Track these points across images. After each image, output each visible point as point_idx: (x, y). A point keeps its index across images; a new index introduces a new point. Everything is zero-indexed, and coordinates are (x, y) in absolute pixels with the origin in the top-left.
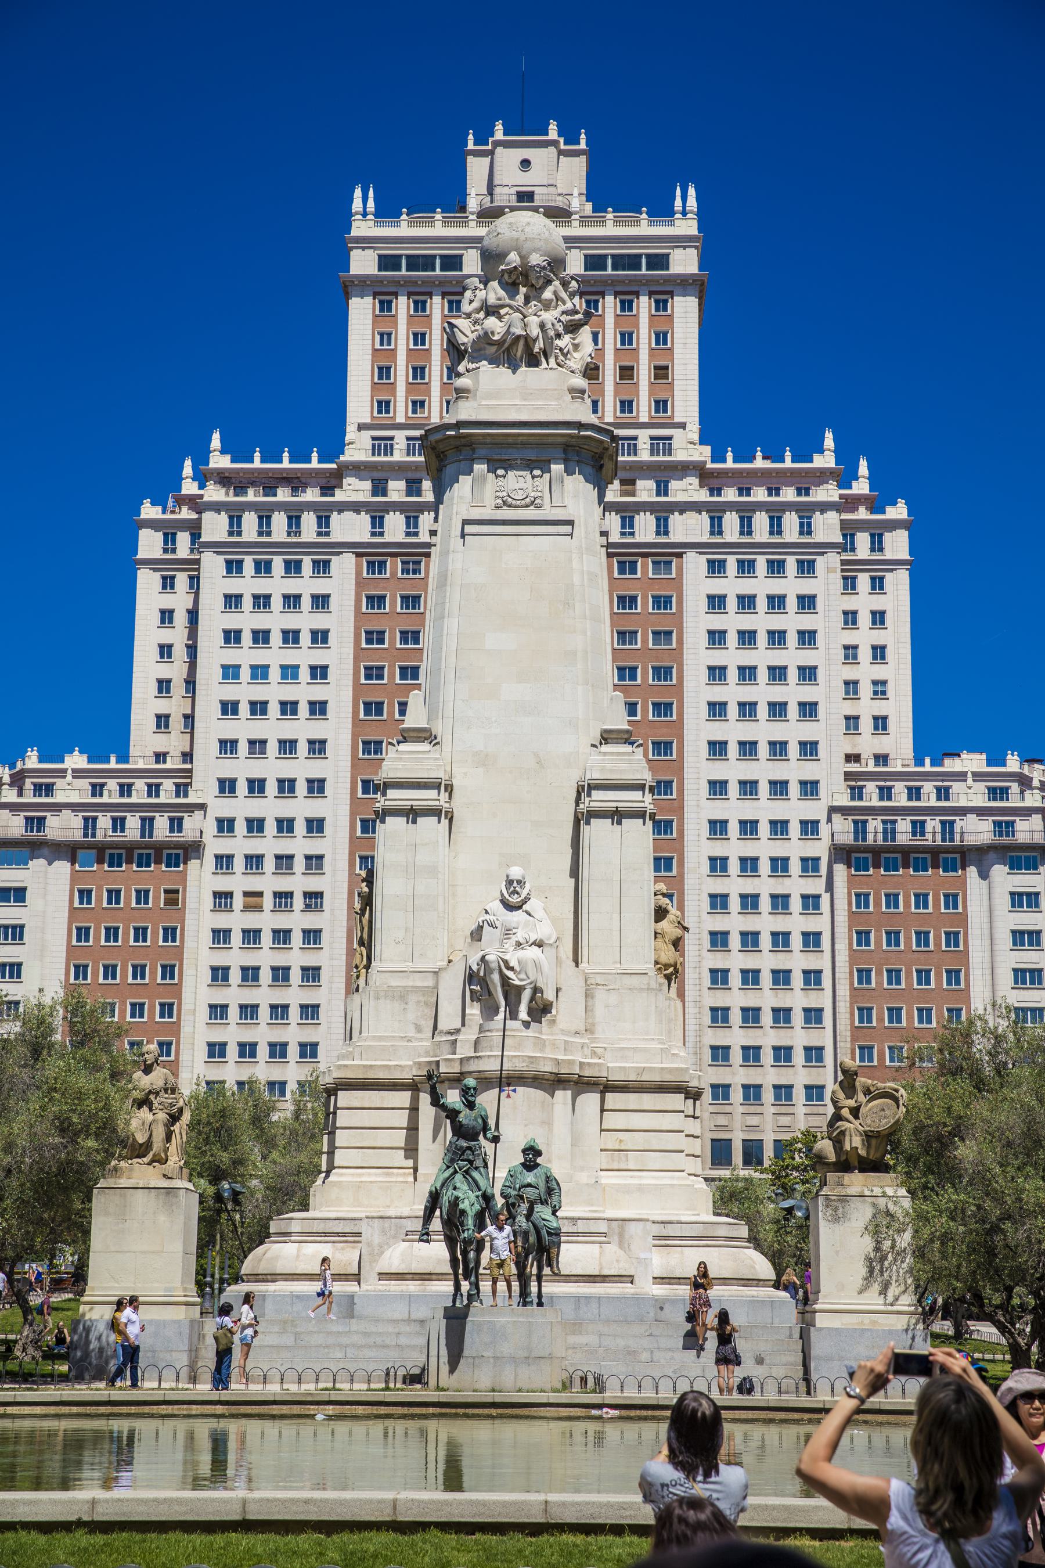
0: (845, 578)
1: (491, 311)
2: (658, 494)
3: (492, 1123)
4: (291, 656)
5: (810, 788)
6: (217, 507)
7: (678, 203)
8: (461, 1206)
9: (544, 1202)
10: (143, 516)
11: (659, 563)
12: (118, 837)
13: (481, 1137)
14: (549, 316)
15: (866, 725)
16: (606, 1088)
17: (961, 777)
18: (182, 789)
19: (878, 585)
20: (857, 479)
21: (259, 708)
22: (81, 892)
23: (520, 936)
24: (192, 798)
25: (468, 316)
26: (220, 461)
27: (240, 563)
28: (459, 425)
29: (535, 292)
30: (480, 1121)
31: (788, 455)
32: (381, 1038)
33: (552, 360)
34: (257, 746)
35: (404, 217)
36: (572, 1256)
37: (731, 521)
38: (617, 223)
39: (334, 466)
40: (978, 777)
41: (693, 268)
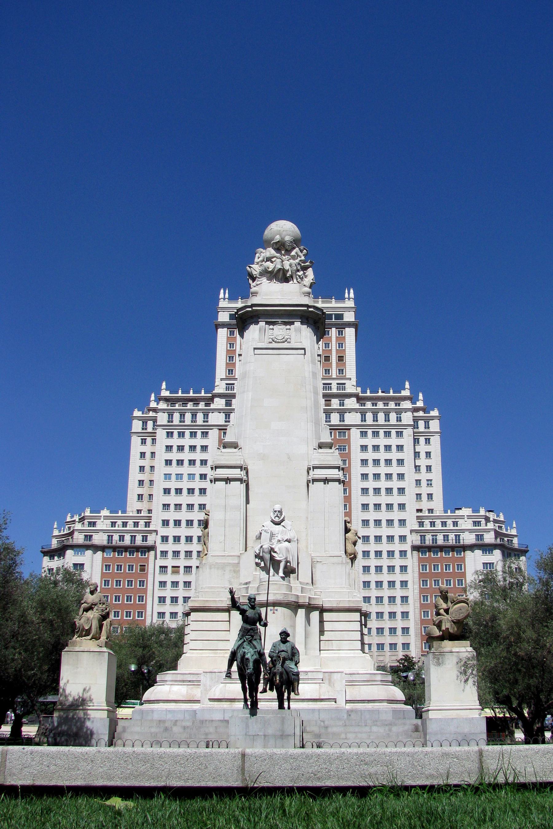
0: (414, 439)
2: (340, 406)
3: (263, 616)
4: (192, 470)
5: (402, 522)
6: (163, 411)
8: (246, 656)
9: (291, 660)
10: (134, 415)
11: (341, 432)
12: (121, 544)
15: (424, 497)
16: (322, 610)
17: (462, 517)
18: (147, 524)
19: (428, 441)
20: (418, 400)
21: (179, 491)
22: (106, 565)
23: (280, 538)
24: (151, 528)
25: (258, 263)
26: (165, 393)
27: (172, 433)
28: (253, 305)
29: (288, 252)
30: (257, 615)
31: (391, 391)
32: (212, 588)
34: (178, 506)
35: (240, 300)
36: (305, 689)
37: (369, 417)
38: (323, 302)
39: (211, 395)
40: (469, 517)
41: (353, 319)
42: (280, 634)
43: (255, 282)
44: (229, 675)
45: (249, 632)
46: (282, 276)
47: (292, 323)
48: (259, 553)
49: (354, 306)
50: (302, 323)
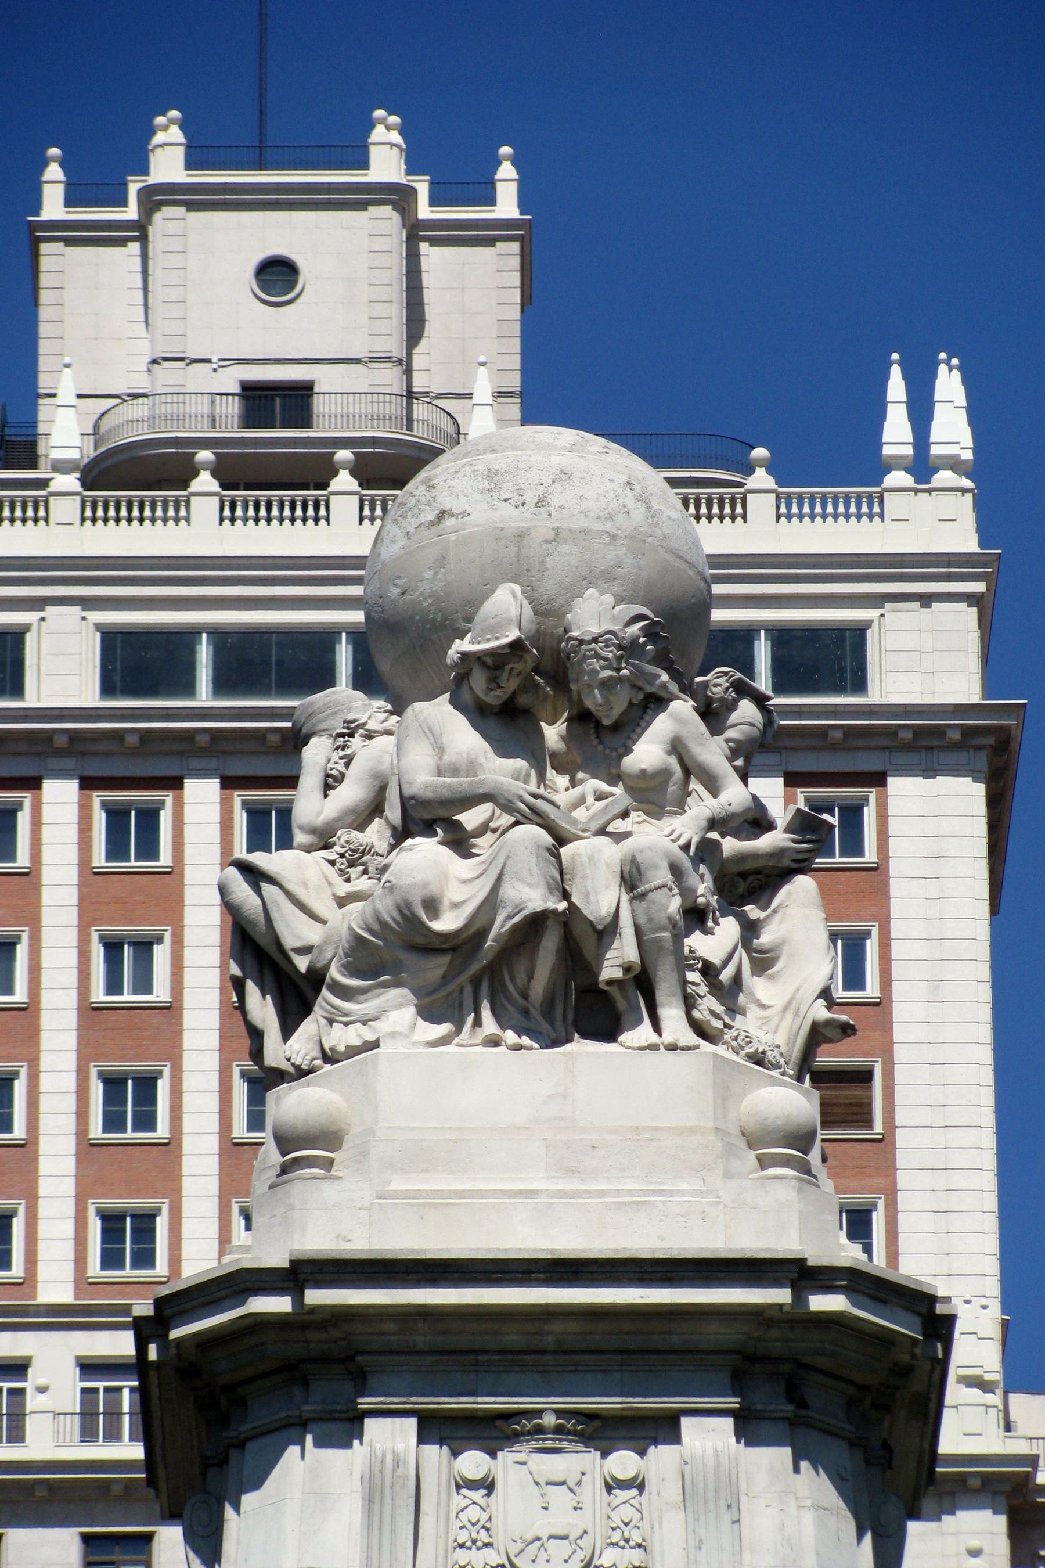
1: (428, 817)
7: (896, 432)
14: (659, 838)
25: (323, 839)
29: (599, 739)
33: (672, 1014)
43: (308, 1028)
49: (968, 543)
50: (750, 1428)
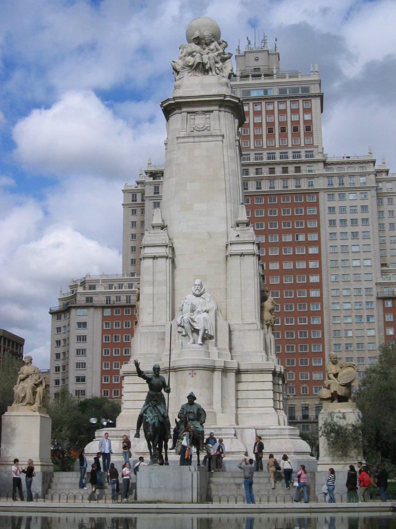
3: (167, 384)
6: (150, 184)
13: (163, 391)
14: (211, 55)
16: (238, 372)
22: (106, 323)
23: (199, 309)
28: (174, 99)
42: (188, 397)
44: (137, 435)
45: (154, 397)
46: (202, 68)
47: (212, 111)
48: (181, 323)
